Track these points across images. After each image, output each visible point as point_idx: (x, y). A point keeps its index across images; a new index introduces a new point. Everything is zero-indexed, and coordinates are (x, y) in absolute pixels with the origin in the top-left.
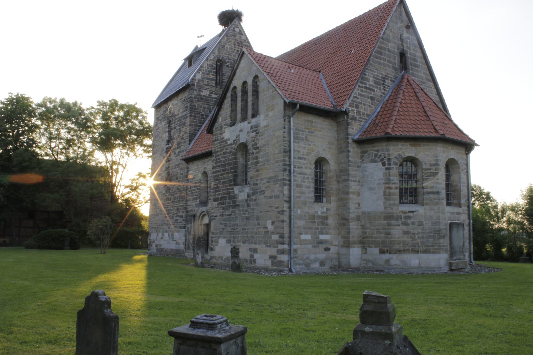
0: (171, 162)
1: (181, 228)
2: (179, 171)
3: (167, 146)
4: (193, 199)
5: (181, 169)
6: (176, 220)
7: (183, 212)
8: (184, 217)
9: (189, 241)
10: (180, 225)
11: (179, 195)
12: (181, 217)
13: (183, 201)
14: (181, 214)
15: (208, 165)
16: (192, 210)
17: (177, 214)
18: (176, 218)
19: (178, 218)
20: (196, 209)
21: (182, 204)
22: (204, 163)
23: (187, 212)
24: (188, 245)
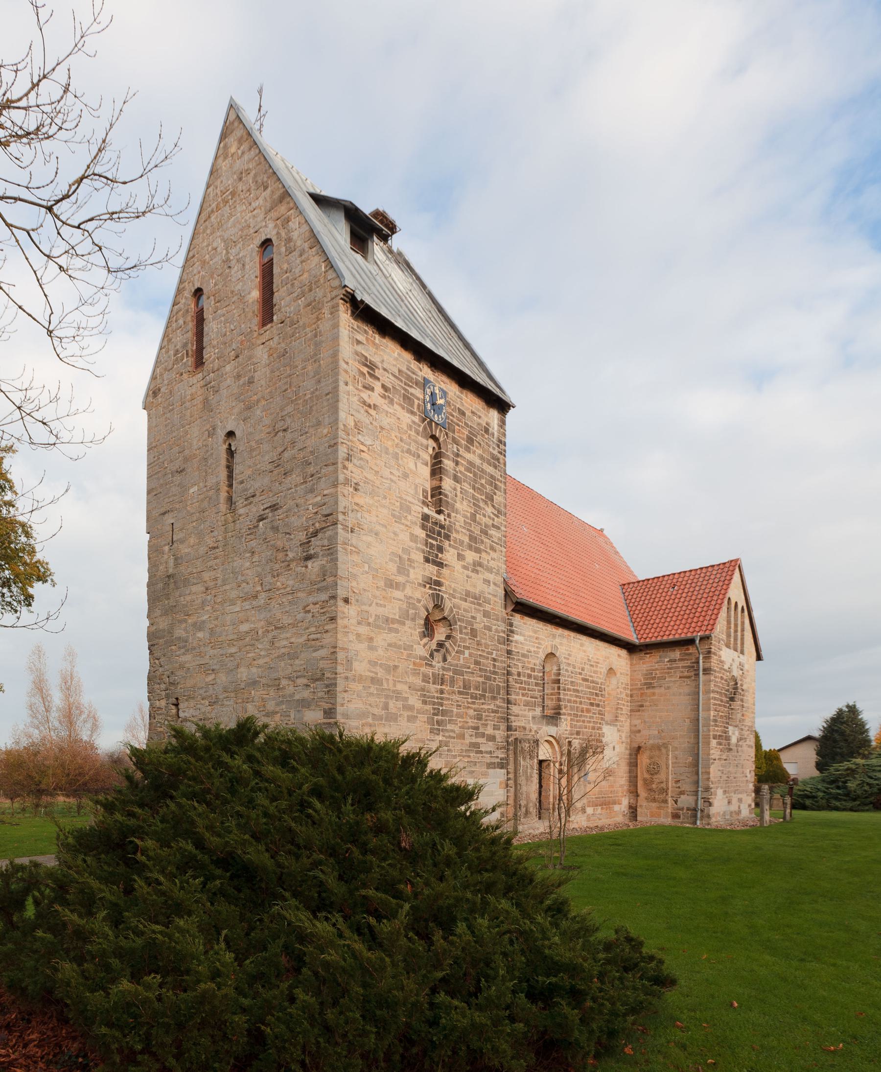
0: (445, 571)
1: (490, 765)
2: (479, 616)
3: (426, 510)
4: (527, 704)
5: (486, 614)
6: (475, 745)
7: (496, 728)
8: (498, 739)
9: (528, 797)
10: (488, 759)
11: (481, 680)
12: (492, 738)
13: (494, 698)
14: (489, 731)
15: (561, 644)
16: (525, 728)
17: (477, 728)
18: (474, 740)
19: (480, 740)
20: (535, 727)
21: (492, 707)
22: (554, 636)
23: (509, 728)
24: (526, 806)
